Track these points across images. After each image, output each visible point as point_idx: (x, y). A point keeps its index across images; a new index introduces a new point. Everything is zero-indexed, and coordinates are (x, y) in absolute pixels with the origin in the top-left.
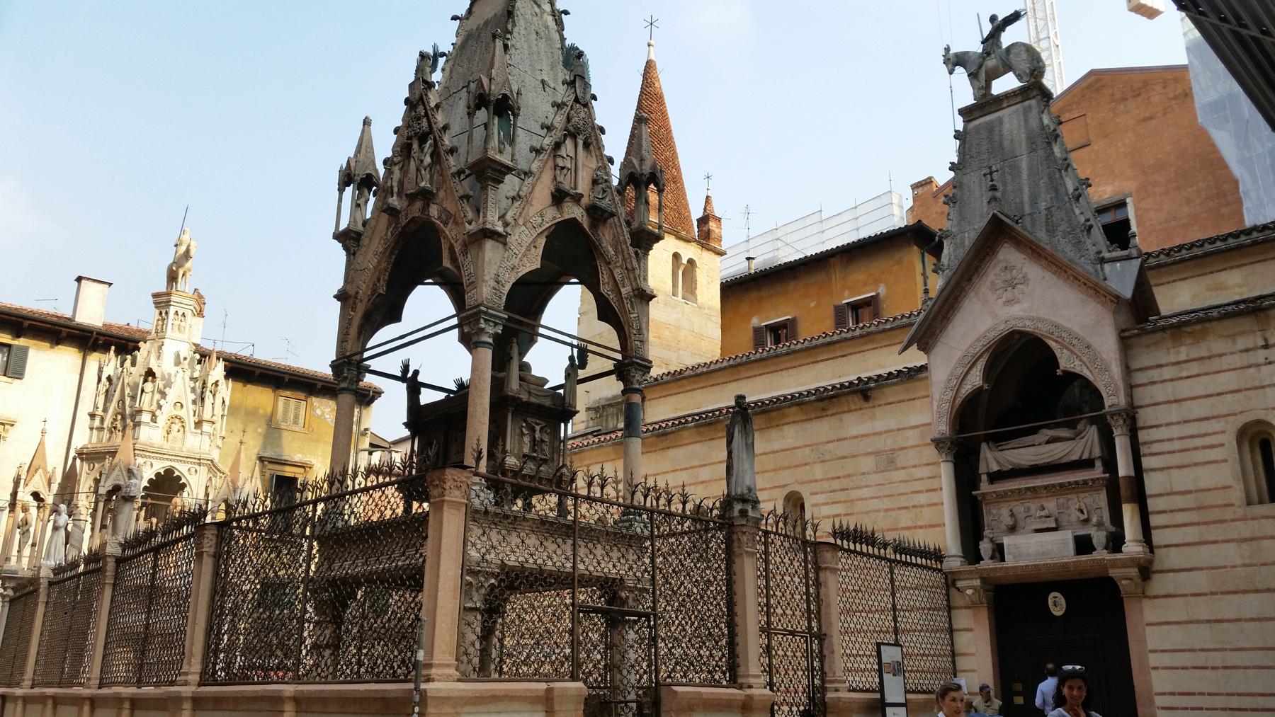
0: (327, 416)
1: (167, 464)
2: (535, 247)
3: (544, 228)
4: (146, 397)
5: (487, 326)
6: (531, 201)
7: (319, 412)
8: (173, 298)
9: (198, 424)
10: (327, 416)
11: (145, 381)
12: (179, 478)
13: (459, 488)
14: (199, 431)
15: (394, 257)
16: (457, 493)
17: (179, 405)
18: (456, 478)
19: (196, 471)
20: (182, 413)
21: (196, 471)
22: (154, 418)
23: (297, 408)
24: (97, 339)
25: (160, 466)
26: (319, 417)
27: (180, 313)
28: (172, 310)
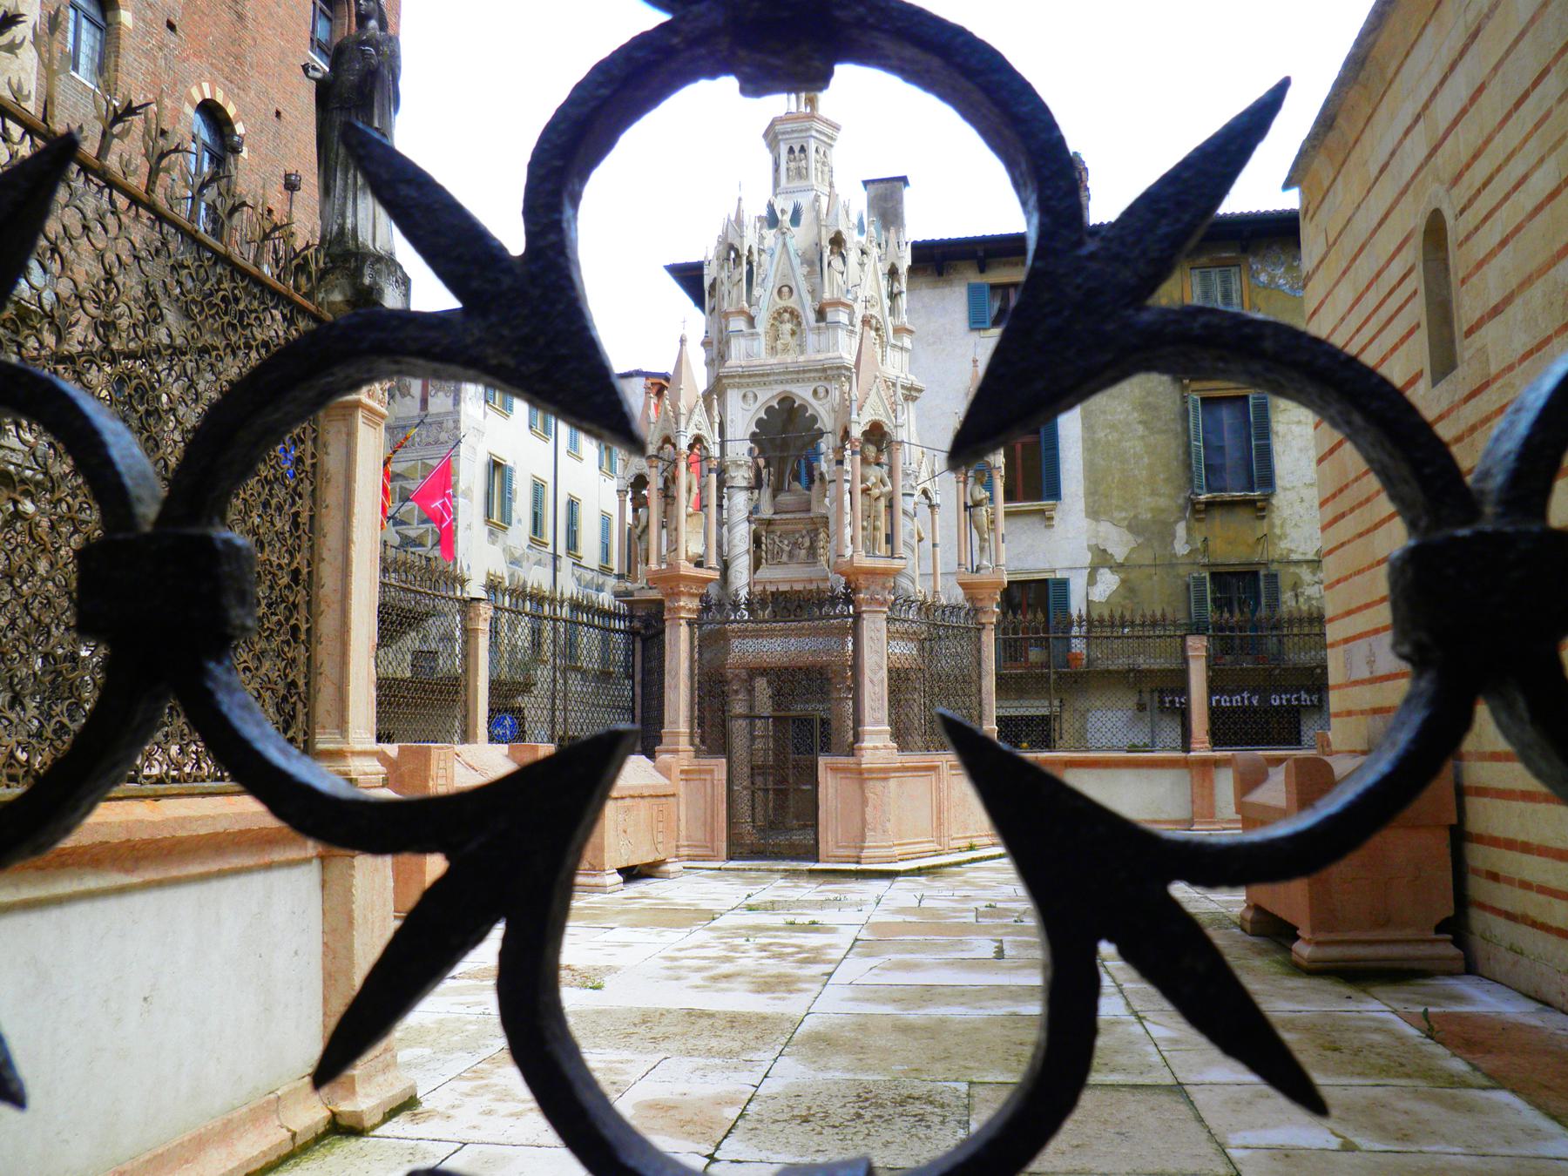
0: (1282, 281)
7: (1263, 278)
9: (821, 315)
10: (1282, 281)
12: (803, 408)
14: (822, 324)
17: (785, 290)
19: (827, 391)
20: (790, 303)
21: (827, 391)
22: (751, 321)
23: (1226, 281)
25: (768, 396)
26: (1266, 287)
27: (797, 149)
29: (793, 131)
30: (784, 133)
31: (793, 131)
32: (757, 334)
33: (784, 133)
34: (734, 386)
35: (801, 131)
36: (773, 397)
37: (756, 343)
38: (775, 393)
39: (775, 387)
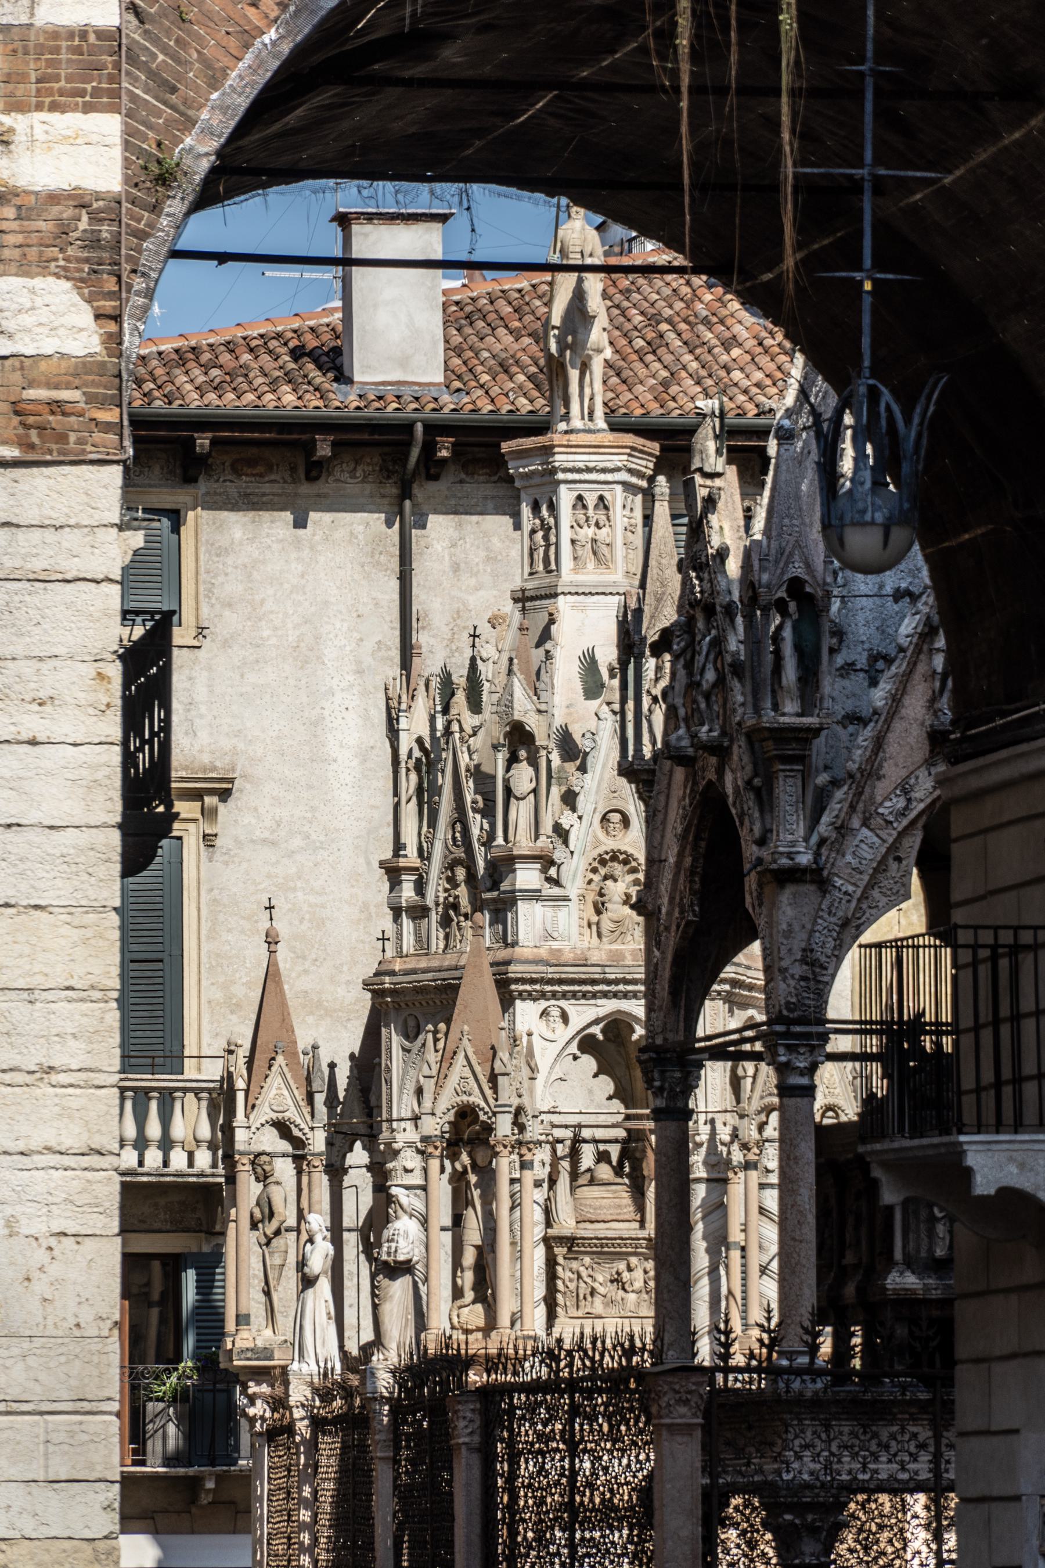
1: (608, 1006)
2: (898, 859)
3: (913, 815)
4: (521, 813)
5: (794, 1056)
6: (881, 766)
8: (560, 459)
11: (513, 760)
13: (686, 1402)
15: (703, 844)
16: (683, 1410)
17: (616, 817)
18: (677, 1387)
24: (429, 448)
27: (591, 499)
28: (566, 497)
29: (589, 470)
30: (566, 470)
31: (589, 470)
32: (566, 899)
33: (566, 470)
34: (530, 997)
35: (604, 471)
36: (596, 1022)
37: (562, 914)
38: (602, 1012)
39: (599, 1002)
